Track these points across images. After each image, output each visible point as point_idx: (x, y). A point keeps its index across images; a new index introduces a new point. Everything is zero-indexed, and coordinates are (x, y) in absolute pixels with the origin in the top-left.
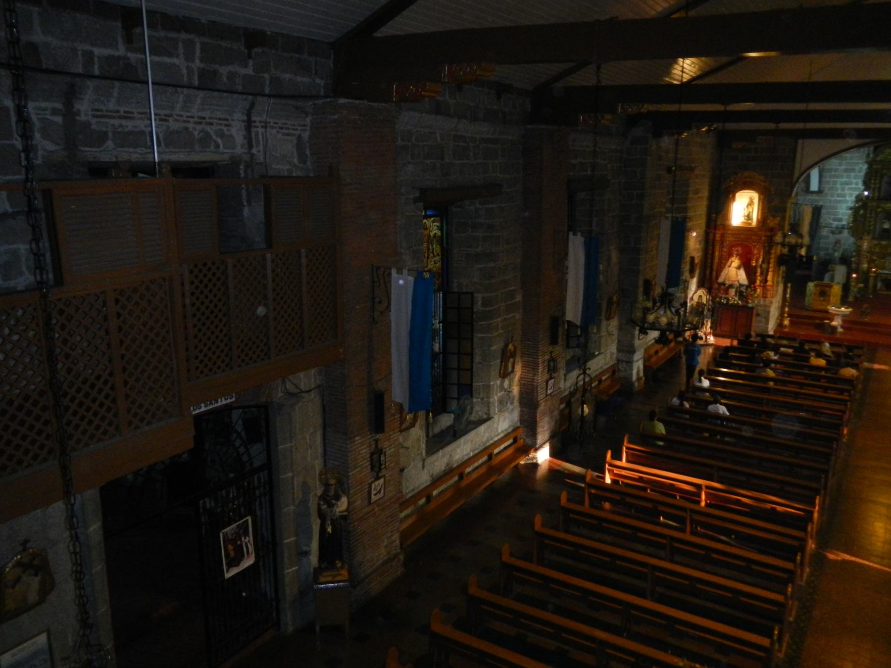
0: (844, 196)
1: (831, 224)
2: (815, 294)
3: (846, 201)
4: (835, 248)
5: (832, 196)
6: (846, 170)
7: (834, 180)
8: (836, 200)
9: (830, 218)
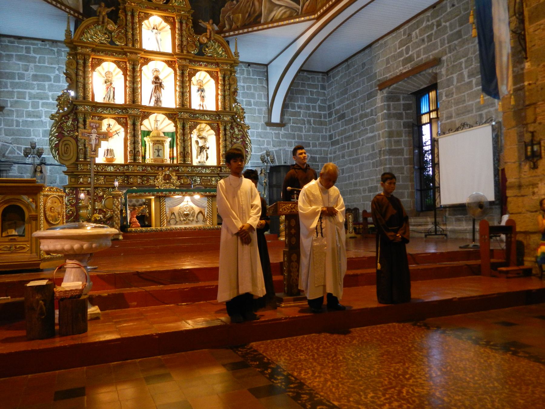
3: (43, 123)
5: (19, 114)
8: (26, 121)
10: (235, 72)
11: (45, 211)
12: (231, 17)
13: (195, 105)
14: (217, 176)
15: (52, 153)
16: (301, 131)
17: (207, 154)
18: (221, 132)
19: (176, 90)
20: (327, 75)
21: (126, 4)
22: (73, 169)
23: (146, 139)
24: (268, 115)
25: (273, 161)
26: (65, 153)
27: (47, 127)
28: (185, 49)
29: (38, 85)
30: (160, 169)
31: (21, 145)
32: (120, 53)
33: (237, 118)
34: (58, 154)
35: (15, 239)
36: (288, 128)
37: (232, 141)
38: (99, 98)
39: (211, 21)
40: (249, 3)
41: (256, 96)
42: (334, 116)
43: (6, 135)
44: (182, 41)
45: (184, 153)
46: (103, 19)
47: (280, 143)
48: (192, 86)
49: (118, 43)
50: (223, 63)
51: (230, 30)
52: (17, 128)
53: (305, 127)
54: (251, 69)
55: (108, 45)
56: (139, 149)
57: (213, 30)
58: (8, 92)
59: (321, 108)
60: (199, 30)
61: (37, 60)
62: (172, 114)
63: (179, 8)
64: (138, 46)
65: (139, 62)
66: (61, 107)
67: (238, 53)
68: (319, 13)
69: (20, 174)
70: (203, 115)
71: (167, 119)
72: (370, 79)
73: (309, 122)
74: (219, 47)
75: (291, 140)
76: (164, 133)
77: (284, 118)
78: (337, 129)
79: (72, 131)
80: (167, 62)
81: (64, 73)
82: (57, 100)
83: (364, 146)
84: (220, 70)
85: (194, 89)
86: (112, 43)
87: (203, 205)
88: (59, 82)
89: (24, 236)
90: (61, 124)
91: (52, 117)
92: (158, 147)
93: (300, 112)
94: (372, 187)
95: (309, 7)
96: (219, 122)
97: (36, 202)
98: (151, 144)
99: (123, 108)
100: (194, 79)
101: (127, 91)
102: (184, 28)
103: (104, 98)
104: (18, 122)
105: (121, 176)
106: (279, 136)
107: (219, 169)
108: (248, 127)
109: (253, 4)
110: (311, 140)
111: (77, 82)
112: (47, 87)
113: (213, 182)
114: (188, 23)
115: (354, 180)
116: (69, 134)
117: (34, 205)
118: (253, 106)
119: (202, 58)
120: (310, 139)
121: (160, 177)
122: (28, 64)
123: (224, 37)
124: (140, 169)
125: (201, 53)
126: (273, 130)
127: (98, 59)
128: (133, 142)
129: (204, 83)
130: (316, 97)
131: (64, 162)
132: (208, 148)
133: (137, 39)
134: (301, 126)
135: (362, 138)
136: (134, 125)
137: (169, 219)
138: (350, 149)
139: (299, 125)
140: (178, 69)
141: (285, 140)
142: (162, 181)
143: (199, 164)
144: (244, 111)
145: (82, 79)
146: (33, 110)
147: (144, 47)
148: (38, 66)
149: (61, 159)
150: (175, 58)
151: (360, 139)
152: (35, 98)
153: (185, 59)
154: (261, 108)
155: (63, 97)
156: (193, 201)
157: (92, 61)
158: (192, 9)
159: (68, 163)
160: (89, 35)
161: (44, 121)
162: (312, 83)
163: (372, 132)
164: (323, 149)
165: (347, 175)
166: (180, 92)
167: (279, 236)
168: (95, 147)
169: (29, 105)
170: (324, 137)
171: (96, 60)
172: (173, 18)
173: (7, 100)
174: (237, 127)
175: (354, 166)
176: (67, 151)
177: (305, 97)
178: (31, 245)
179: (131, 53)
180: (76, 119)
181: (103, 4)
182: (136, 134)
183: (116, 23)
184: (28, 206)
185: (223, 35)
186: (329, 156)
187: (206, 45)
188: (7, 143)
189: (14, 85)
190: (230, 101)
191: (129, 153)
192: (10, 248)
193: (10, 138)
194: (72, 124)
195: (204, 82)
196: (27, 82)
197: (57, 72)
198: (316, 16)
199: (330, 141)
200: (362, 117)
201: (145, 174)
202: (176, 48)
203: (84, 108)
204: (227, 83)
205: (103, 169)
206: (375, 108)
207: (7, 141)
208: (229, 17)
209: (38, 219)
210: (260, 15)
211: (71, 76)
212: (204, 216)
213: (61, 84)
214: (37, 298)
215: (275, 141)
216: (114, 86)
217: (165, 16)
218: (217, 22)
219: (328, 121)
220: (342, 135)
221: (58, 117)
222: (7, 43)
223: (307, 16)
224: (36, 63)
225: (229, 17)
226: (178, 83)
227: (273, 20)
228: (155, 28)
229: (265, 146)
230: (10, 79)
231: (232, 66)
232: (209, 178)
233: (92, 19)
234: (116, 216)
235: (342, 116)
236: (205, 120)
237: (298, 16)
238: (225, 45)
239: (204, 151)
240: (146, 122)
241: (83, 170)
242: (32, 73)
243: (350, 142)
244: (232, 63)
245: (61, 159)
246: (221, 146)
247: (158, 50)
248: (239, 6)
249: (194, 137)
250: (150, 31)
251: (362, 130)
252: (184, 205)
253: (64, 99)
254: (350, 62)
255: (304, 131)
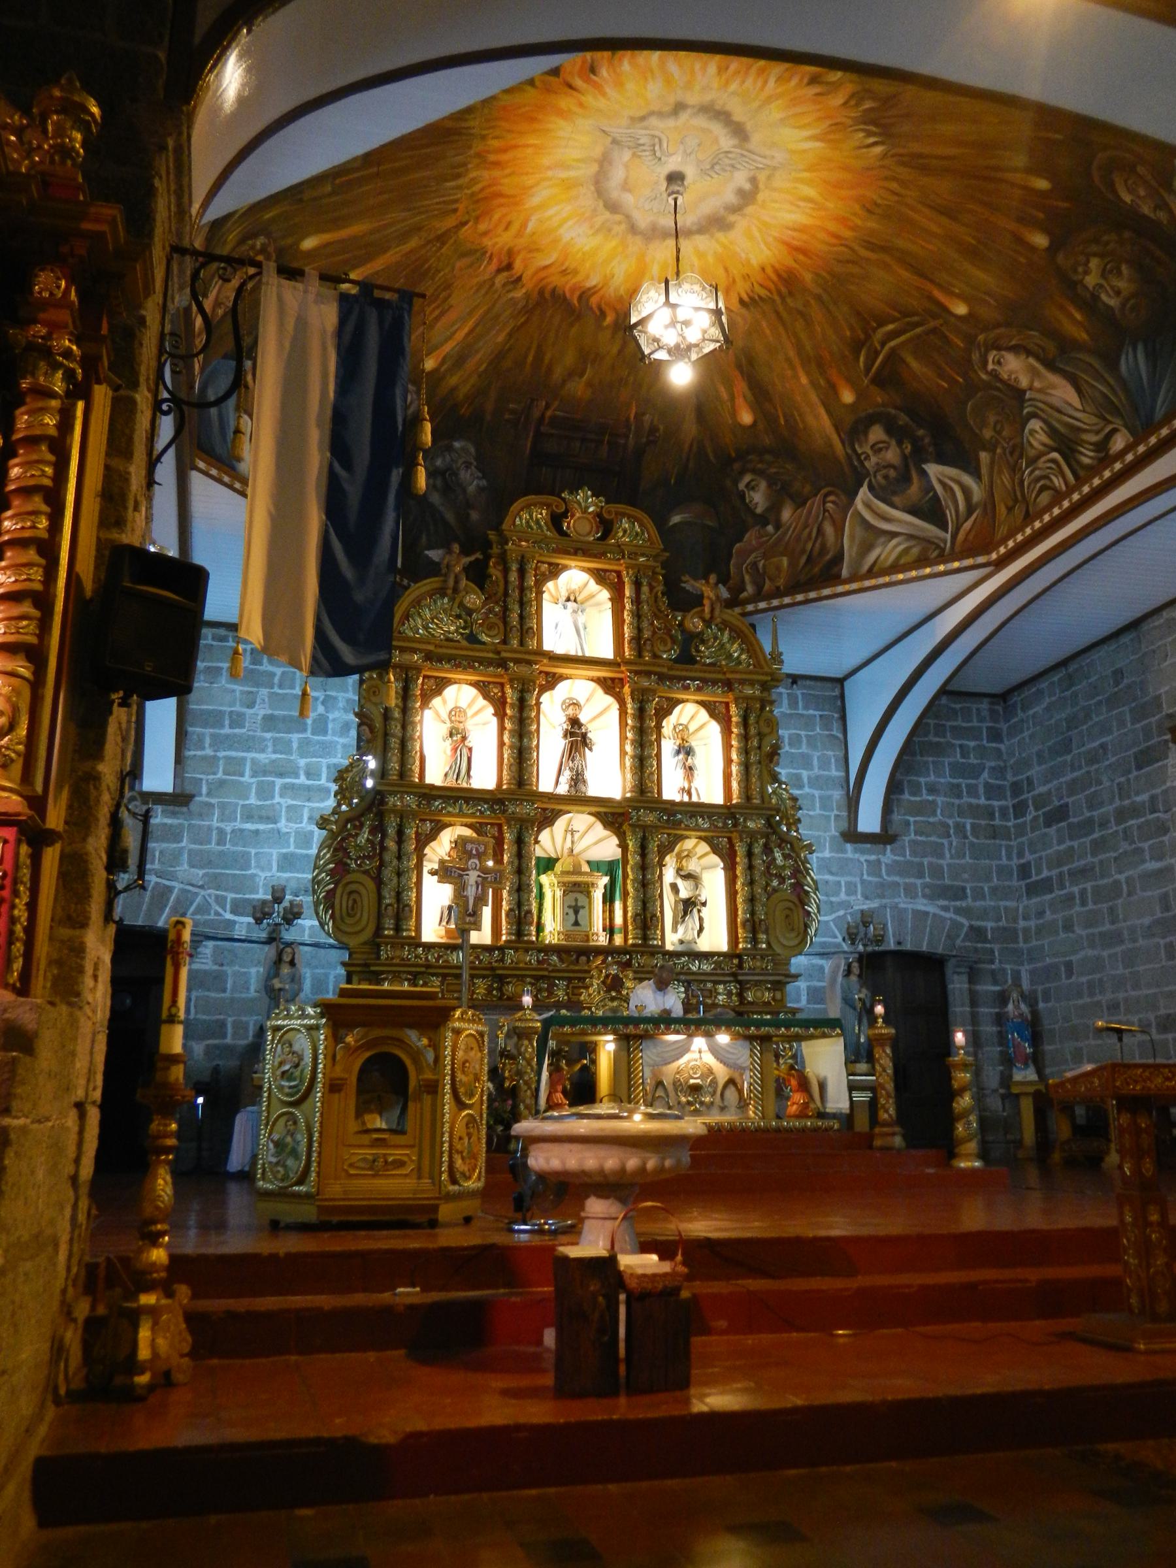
0: (275, 821)
1: (231, 924)
2: (334, 1087)
3: (279, 837)
4: (277, 984)
6: (270, 722)
7: (233, 754)
8: (242, 831)
9: (220, 901)
10: (772, 703)
11: (453, 1069)
12: (761, 564)
13: (671, 789)
14: (730, 982)
15: (317, 914)
16: (941, 856)
17: (701, 919)
18: (738, 859)
19: (623, 753)
20: (1005, 702)
21: (507, 543)
22: (365, 956)
23: (544, 879)
24: (849, 812)
25: (880, 939)
26: (349, 915)
27: (289, 847)
28: (648, 648)
29: (275, 740)
30: (583, 959)
31: (226, 890)
32: (490, 663)
33: (779, 823)
34: (332, 917)
35: (384, 1140)
36: (903, 848)
37: (768, 885)
38: (435, 775)
39: (713, 578)
40: (807, 530)
41: (815, 762)
42: (1031, 813)
43: (192, 866)
44: (639, 630)
45: (645, 918)
46: (457, 582)
47: (881, 890)
48: (664, 742)
49: (485, 638)
50: (742, 682)
51: (759, 596)
52: (221, 848)
53: (951, 844)
54: (799, 692)
55: (464, 643)
56: (530, 905)
57: (718, 597)
58: (204, 758)
59: (992, 791)
60: (684, 602)
61: (276, 680)
62: (613, 814)
63: (633, 549)
64: (533, 644)
65: (535, 683)
66: (344, 797)
67: (781, 654)
68: (1002, 550)
69: (216, 967)
70: (693, 815)
71: (599, 826)
72: (1141, 713)
73: (960, 828)
74: (732, 640)
75: (912, 880)
76: (588, 862)
77: (890, 821)
78: (1045, 850)
79: (369, 857)
80: (600, 682)
81: (356, 715)
82: (335, 781)
83: (1136, 897)
84: (736, 700)
85: (668, 746)
86: (472, 639)
87: (739, 1062)
88: (324, 732)
89: (402, 1132)
90: (343, 840)
91: (323, 823)
92: (576, 900)
93: (934, 802)
94: (1169, 1016)
95: (971, 537)
96: (735, 835)
97: (436, 1046)
98: (559, 893)
99: (493, 800)
100: (668, 724)
101: (506, 756)
102: (643, 597)
103: (446, 775)
104: (221, 832)
105: (484, 977)
106: (881, 870)
107: (736, 961)
108: (810, 845)
109: (820, 531)
110: (967, 881)
111: (386, 735)
112: (295, 745)
113: (720, 998)
114: (654, 584)
115: (1109, 996)
116: (359, 866)
117: (430, 1056)
118: (807, 790)
119: (691, 671)
120: (966, 876)
121: (595, 982)
122: (254, 689)
123: (744, 615)
124: (532, 958)
125: (686, 658)
126: (863, 852)
127: (436, 678)
128: (515, 887)
129: (691, 730)
130: (975, 762)
131: (345, 939)
132: (704, 904)
133: (532, 628)
134: (940, 841)
135: (1126, 874)
136: (520, 842)
137: (649, 1097)
138: (1090, 906)
139: (933, 839)
140: (629, 700)
141: (897, 879)
142: (599, 993)
143: (680, 948)
144: (800, 802)
145: (399, 727)
146: (259, 803)
147: (547, 647)
148: (278, 694)
149: (340, 930)
150: (622, 672)
151: (1122, 877)
152: (265, 773)
153: (648, 674)
154: (830, 792)
155: (351, 774)
156: (715, 1050)
157: (423, 684)
158: (665, 550)
159: (353, 942)
160: (419, 621)
161: (284, 830)
162: (964, 725)
163: (1161, 858)
164: (1002, 903)
165: (1084, 979)
166: (633, 757)
167: (952, 1155)
168: (475, 905)
169: (250, 789)
170: (1003, 871)
171: (432, 681)
172: (619, 574)
173: (201, 779)
174: (779, 846)
175: (1105, 954)
176: (353, 908)
177: (947, 760)
178: (420, 1156)
179: (517, 661)
180: (379, 829)
181: (456, 548)
182: (524, 865)
183: (482, 588)
184: (416, 1055)
185: (738, 610)
186: (1022, 924)
187: (700, 638)
188: (192, 885)
189: (219, 742)
190: (760, 777)
191: (507, 915)
192: (374, 1161)
193: (201, 872)
194: (368, 839)
195: (692, 728)
196: (251, 733)
197: (321, 709)
198: (994, 556)
199: (1023, 883)
200: (1122, 815)
201: (546, 973)
202: (626, 645)
203: (402, 799)
204: (753, 731)
205: (440, 957)
206: (1165, 792)
207: (194, 882)
208: (755, 564)
209: (440, 1090)
210: (839, 558)
211: (372, 720)
212: (740, 1091)
213: (328, 738)
214: (592, 1288)
215: (870, 882)
216: (470, 745)
217: (598, 570)
218: (724, 579)
219: (1015, 826)
220: (1059, 865)
221: (336, 822)
222: (210, 642)
223: (968, 557)
224: (272, 688)
225: (755, 564)
226: (630, 735)
227: (876, 569)
228: (572, 598)
229: (843, 896)
230: (213, 727)
231: (765, 687)
232: (709, 985)
233: (429, 584)
234: (525, 1088)
235: (1060, 814)
236: (697, 828)
237: (943, 558)
238: (746, 637)
239: (695, 911)
240: (544, 836)
241: (392, 958)
242: (262, 712)
243: (1088, 886)
244: (766, 682)
245: (340, 930)
246: (740, 899)
247: (580, 654)
248: (780, 539)
249: (669, 875)
250: (560, 605)
251: (1126, 852)
252: (689, 1062)
253: (352, 778)
254: (1072, 667)
255: (948, 855)
